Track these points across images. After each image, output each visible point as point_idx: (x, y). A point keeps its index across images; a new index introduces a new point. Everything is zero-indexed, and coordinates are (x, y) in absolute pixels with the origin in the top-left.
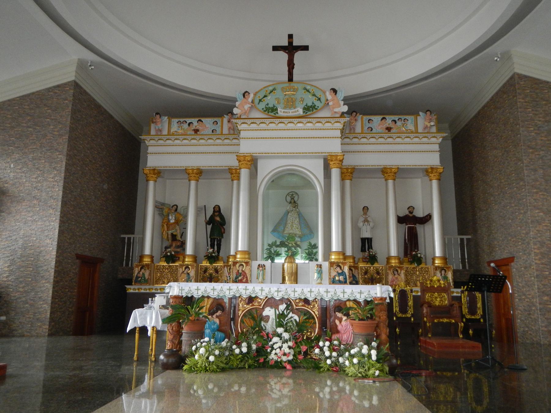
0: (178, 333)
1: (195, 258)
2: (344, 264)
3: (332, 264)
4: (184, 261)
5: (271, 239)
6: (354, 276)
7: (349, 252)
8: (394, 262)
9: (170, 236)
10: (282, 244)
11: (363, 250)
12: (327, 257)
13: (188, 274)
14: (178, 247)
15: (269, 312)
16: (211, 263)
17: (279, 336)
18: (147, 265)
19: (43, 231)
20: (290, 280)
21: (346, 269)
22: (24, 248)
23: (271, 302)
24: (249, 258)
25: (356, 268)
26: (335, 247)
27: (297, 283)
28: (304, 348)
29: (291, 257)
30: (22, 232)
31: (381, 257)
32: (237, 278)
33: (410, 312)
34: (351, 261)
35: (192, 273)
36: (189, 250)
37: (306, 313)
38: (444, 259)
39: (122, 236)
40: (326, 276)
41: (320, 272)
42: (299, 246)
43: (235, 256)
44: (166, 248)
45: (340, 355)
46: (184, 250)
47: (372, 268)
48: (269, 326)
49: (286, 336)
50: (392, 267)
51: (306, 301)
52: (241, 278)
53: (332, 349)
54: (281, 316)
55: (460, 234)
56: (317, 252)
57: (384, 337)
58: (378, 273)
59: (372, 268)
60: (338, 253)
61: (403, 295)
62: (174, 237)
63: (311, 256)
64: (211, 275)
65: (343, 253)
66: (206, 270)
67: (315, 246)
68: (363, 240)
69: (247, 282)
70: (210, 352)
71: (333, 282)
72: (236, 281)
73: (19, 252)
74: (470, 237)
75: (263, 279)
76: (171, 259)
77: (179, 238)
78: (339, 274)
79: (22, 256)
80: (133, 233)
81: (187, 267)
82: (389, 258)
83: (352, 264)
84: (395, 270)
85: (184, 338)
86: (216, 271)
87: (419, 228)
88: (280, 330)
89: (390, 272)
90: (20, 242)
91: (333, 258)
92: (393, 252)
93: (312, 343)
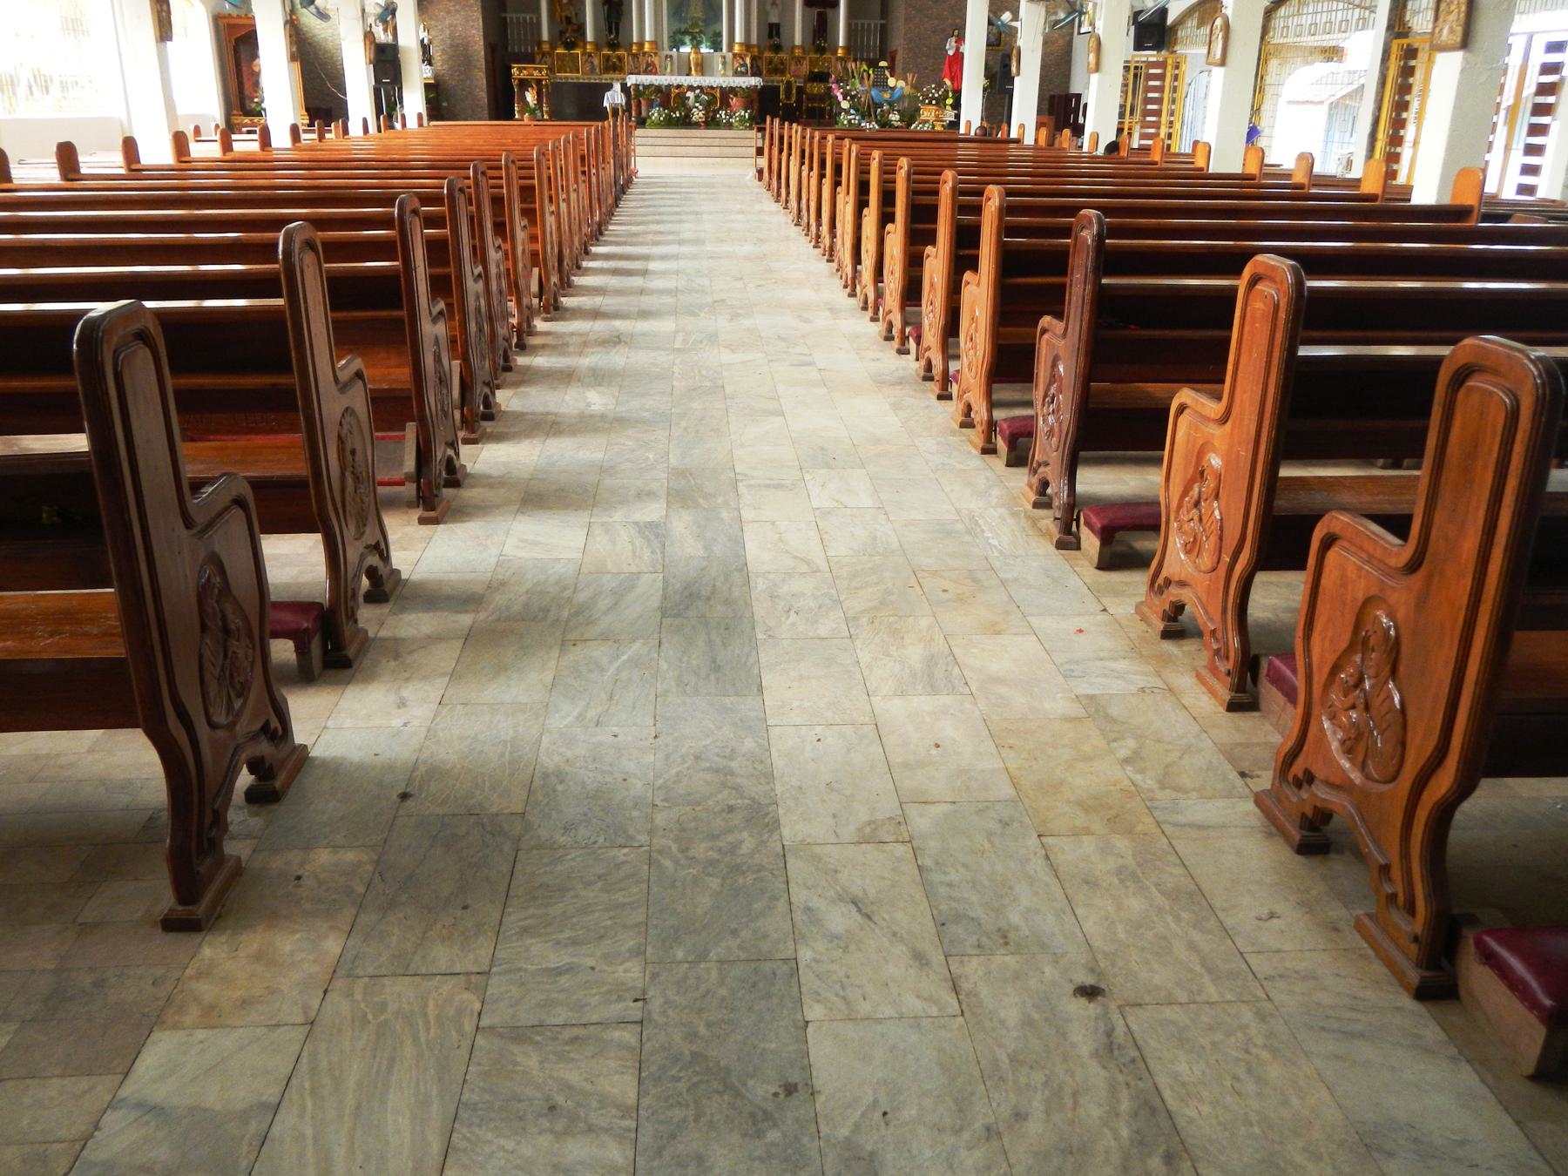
0: (639, 105)
1: (597, 46)
2: (746, 56)
3: (735, 55)
4: (585, 48)
5: (676, 26)
6: (758, 67)
7: (754, 40)
8: (798, 52)
9: (564, 19)
10: (686, 33)
11: (770, 36)
12: (730, 48)
13: (592, 63)
14: (574, 31)
15: (690, 94)
16: (614, 51)
17: (697, 108)
18: (548, 53)
19: (467, 21)
20: (696, 70)
21: (748, 61)
22: (452, 37)
23: (691, 88)
24: (656, 49)
25: (760, 58)
26: (739, 37)
27: (703, 75)
28: (711, 114)
29: (696, 46)
30: (447, 22)
31: (785, 43)
32: (647, 68)
33: (794, 99)
34: (756, 50)
35: (596, 62)
36: (590, 36)
37: (712, 95)
38: (848, 49)
39: (503, 15)
40: (729, 67)
41: (724, 64)
42: (701, 32)
43: (641, 45)
44: (562, 33)
45: (731, 117)
46: (584, 34)
47: (776, 57)
48: (691, 102)
49: (701, 107)
50: (795, 57)
51: (712, 88)
52: (650, 70)
53: (726, 114)
54: (697, 97)
55: (882, 18)
56: (721, 41)
57: (755, 107)
58: (782, 63)
59: (776, 57)
60: (740, 44)
61: (789, 83)
62: (568, 20)
63: (716, 46)
64: (614, 63)
65: (747, 46)
66: (607, 58)
67: (720, 35)
68: (771, 26)
69: (655, 73)
70: (660, 115)
71: (736, 73)
72: (646, 72)
73: (449, 42)
74: (883, 22)
75: (671, 70)
76: (570, 46)
77: (574, 20)
78: (741, 66)
79: (452, 46)
80: (505, 11)
81: (590, 55)
82: (794, 47)
83: (756, 54)
84: (799, 60)
85: (643, 108)
86: (620, 59)
87: (829, 12)
88: (697, 105)
89: (793, 63)
90: (448, 32)
91: (737, 49)
92: (798, 41)
93: (715, 112)
